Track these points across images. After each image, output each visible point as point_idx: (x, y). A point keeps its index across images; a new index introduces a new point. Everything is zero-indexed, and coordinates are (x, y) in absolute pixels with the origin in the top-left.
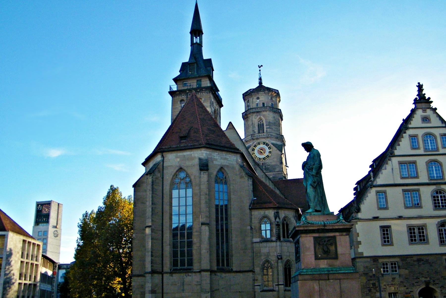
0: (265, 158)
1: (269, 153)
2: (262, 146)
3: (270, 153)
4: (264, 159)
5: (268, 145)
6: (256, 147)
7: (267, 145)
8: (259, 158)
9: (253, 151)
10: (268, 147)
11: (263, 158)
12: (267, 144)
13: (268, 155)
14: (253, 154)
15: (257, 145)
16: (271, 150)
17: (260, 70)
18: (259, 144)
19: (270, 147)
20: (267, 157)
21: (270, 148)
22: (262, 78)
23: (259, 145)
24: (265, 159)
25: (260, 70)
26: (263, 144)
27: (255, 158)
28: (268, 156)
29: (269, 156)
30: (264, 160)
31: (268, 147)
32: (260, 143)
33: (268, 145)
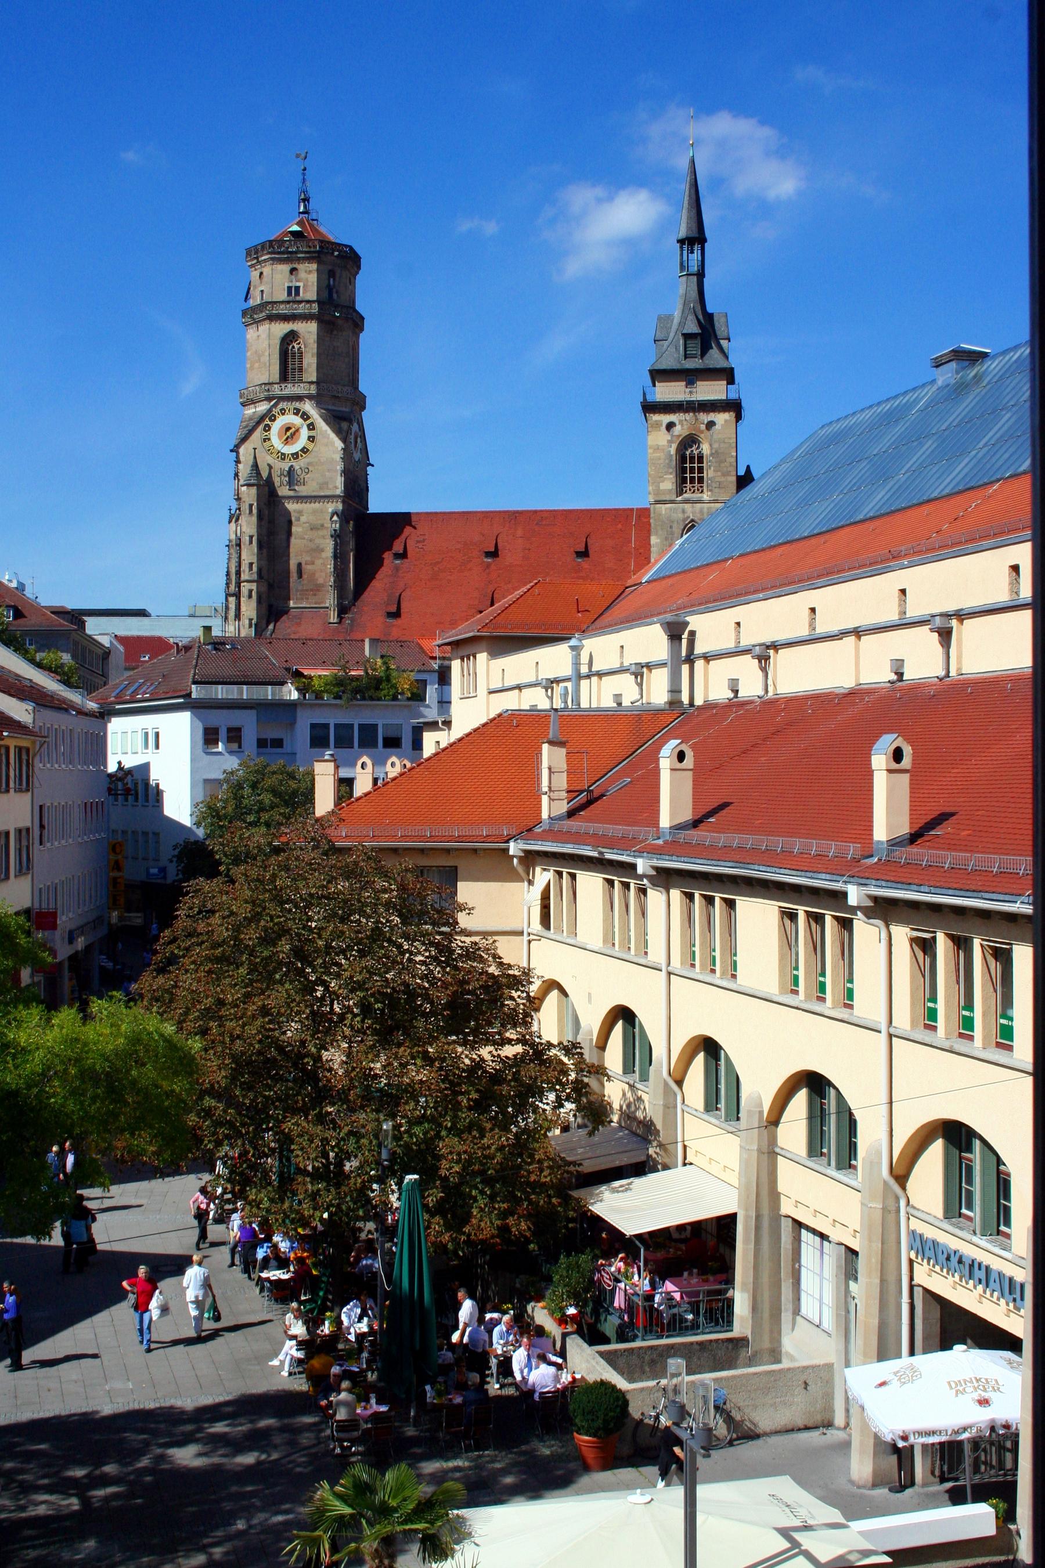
0: (297, 453)
3: (313, 441)
4: (295, 456)
5: (308, 418)
8: (283, 454)
9: (266, 431)
10: (308, 422)
11: (293, 455)
12: (304, 413)
14: (265, 440)
18: (283, 412)
19: (312, 424)
21: (311, 427)
22: (311, 193)
24: (297, 457)
28: (304, 450)
31: (308, 422)
33: (308, 418)
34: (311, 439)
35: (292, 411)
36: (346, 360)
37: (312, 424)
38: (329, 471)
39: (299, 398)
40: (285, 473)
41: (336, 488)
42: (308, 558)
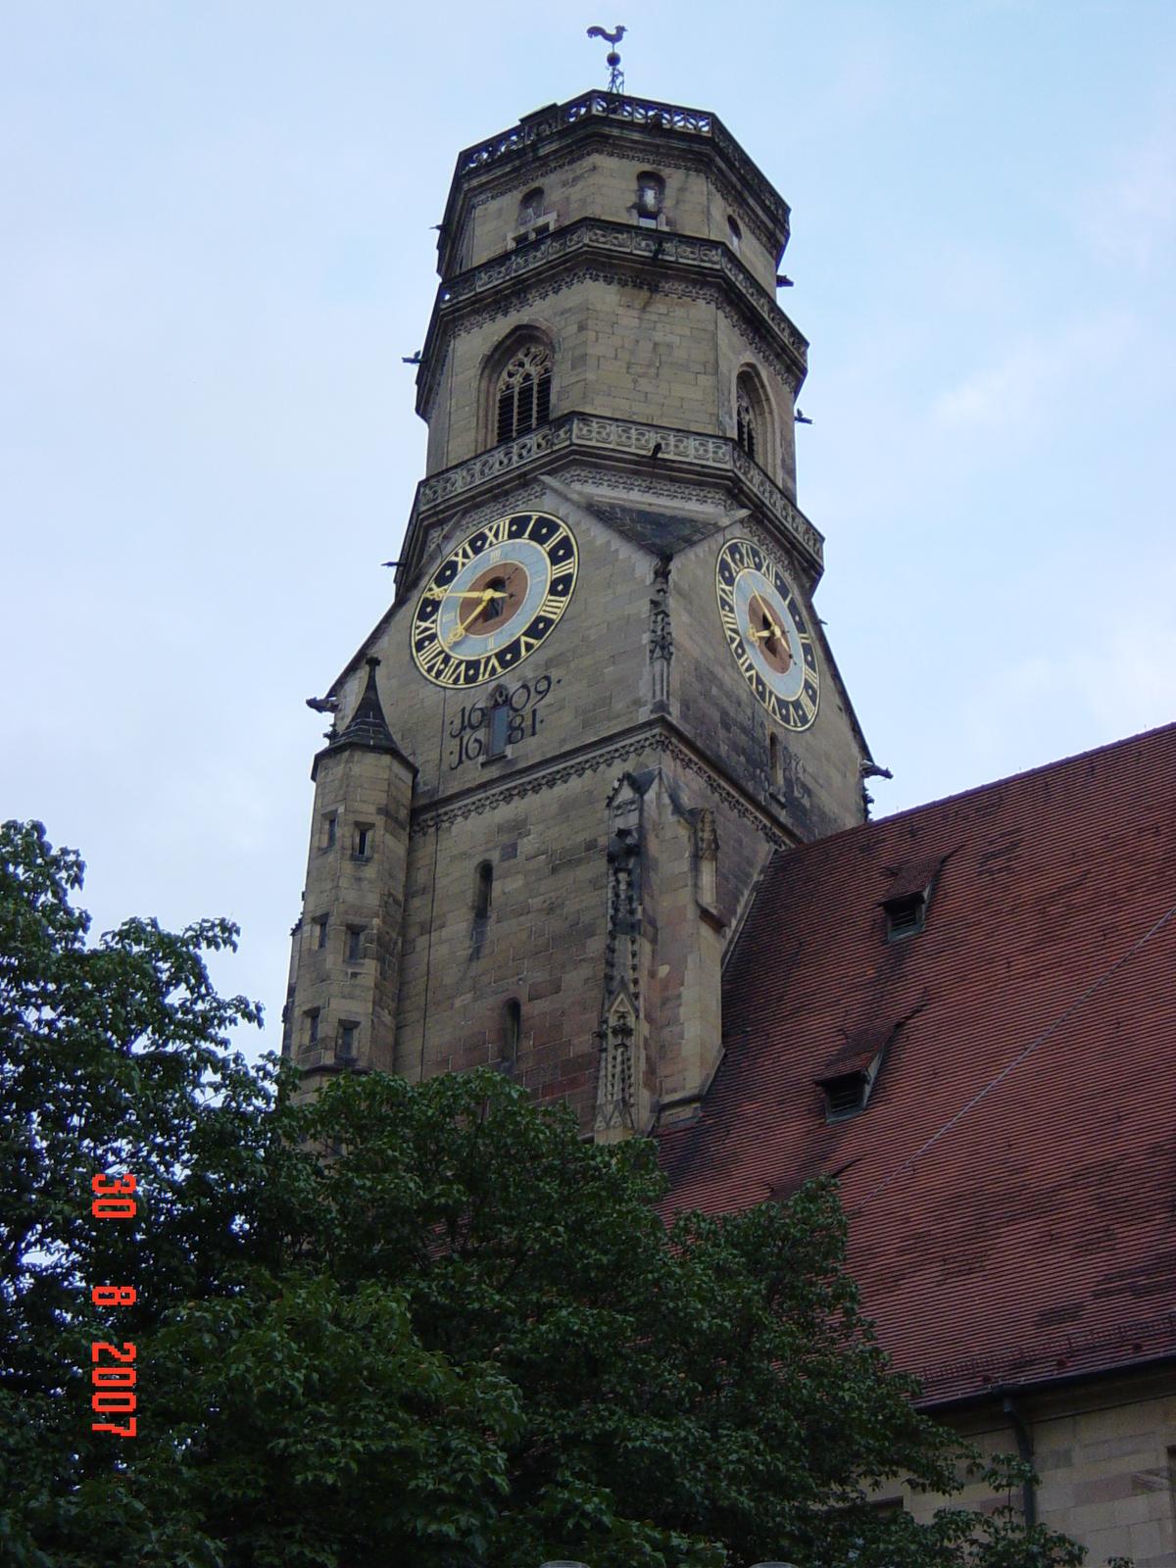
0: (514, 648)
1: (553, 591)
2: (501, 551)
3: (564, 593)
4: (509, 655)
6: (454, 574)
7: (543, 530)
8: (473, 665)
9: (423, 616)
13: (539, 619)
15: (460, 559)
16: (569, 567)
17: (613, 60)
18: (478, 544)
19: (565, 543)
20: (533, 631)
23: (477, 551)
24: (516, 656)
25: (613, 60)
26: (512, 535)
27: (439, 673)
28: (538, 628)
29: (549, 622)
30: (504, 664)
32: (483, 537)
33: (553, 528)
34: (560, 586)
35: (504, 533)
36: (704, 380)
37: (565, 543)
38: (613, 659)
39: (524, 481)
40: (476, 717)
41: (638, 703)
42: (540, 976)
